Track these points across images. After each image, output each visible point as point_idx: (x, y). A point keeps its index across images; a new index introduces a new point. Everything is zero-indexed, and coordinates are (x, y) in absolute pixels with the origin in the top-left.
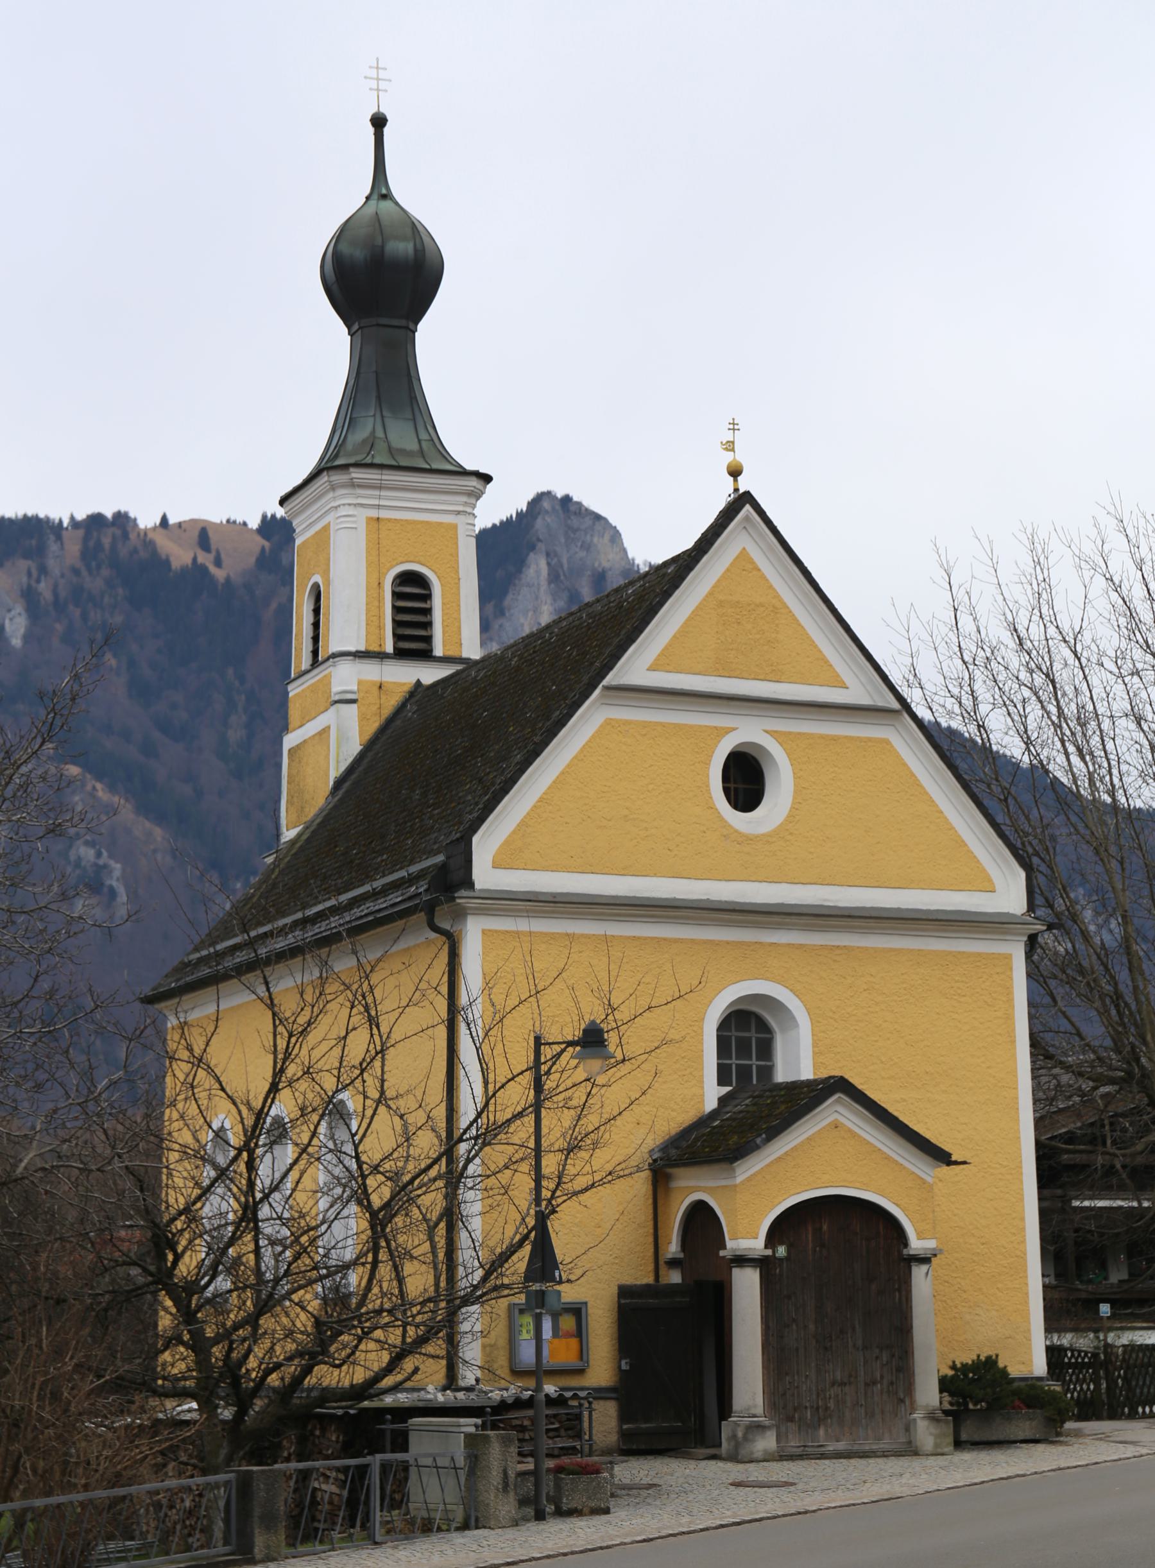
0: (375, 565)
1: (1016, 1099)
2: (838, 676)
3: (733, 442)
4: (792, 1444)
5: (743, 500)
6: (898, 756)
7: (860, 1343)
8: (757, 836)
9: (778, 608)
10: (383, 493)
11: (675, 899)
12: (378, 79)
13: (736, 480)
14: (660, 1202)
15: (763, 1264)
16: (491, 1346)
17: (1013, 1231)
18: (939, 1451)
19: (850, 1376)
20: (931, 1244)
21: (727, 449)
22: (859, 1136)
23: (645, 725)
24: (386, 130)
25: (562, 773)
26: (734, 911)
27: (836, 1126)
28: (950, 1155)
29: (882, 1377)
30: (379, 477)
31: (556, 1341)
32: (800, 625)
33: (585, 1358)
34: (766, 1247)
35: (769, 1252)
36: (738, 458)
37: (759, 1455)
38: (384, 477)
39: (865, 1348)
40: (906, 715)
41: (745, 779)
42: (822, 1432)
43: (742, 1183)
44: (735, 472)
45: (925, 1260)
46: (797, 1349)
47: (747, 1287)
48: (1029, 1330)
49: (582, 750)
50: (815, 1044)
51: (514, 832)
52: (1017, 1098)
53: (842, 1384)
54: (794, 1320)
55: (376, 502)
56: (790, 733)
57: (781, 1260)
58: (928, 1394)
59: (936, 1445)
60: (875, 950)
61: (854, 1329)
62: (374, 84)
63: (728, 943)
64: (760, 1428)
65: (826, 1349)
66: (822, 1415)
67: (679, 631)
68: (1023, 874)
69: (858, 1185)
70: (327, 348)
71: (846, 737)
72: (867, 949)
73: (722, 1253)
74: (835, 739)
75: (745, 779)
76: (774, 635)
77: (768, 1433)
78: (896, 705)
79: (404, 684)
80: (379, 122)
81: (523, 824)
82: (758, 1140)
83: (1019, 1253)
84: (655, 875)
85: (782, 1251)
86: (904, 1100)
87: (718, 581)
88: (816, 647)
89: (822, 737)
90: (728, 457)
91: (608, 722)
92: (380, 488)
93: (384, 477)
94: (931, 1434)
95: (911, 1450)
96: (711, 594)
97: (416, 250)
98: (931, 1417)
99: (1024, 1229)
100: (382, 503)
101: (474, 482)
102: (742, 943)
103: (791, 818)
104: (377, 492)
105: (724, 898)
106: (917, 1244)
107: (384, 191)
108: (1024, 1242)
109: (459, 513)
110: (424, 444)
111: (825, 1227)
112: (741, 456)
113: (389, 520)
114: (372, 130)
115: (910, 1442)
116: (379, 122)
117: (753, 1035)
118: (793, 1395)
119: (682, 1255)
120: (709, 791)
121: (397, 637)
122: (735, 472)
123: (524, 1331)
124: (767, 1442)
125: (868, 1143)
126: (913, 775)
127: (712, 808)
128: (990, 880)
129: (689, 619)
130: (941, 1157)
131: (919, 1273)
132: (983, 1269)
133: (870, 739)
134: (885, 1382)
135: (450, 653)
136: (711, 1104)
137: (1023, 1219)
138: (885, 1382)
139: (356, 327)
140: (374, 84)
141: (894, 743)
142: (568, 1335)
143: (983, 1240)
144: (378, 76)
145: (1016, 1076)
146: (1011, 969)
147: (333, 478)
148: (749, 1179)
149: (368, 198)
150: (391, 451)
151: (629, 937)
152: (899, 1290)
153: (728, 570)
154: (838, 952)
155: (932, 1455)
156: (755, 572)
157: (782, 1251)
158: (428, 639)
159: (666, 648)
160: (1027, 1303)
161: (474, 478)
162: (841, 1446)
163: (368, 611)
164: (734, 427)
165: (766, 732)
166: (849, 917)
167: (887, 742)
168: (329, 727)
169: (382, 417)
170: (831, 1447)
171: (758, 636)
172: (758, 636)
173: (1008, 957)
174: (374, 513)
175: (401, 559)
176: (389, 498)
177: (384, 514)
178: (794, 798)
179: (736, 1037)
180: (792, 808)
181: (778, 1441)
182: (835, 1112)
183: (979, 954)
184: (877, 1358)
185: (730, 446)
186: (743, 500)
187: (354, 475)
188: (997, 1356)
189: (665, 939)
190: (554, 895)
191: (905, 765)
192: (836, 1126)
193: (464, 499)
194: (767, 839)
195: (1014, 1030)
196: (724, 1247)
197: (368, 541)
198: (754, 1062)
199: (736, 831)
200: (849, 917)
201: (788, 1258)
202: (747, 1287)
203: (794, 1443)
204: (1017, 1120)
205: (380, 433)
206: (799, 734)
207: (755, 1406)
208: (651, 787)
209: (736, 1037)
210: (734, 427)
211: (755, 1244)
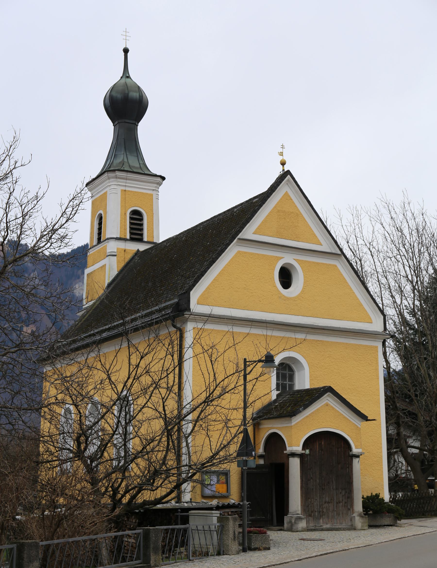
0: (124, 206)
1: (379, 399)
2: (319, 241)
3: (282, 153)
4: (311, 525)
5: (286, 174)
6: (340, 271)
7: (335, 487)
8: (291, 298)
9: (298, 214)
10: (127, 181)
11: (262, 320)
12: (126, 36)
13: (283, 167)
14: (256, 433)
15: (301, 456)
18: (363, 528)
19: (331, 500)
20: (360, 450)
21: (280, 155)
24: (129, 54)
25: (222, 270)
27: (327, 405)
28: (367, 417)
29: (342, 500)
32: (306, 221)
33: (229, 492)
34: (302, 450)
35: (303, 452)
37: (300, 529)
39: (336, 489)
41: (286, 277)
42: (321, 521)
43: (294, 425)
44: (283, 164)
45: (357, 456)
46: (313, 489)
47: (295, 465)
49: (229, 262)
50: (310, 376)
51: (205, 291)
52: (379, 399)
53: (328, 503)
54: (312, 478)
55: (125, 184)
56: (303, 261)
57: (307, 455)
58: (358, 507)
59: (362, 526)
61: (333, 482)
62: (125, 37)
64: (299, 519)
65: (323, 489)
66: (321, 514)
67: (264, 220)
69: (335, 427)
70: (105, 130)
71: (322, 263)
72: (328, 342)
73: (285, 452)
75: (286, 277)
78: (339, 252)
79: (133, 250)
80: (126, 51)
81: (208, 288)
82: (301, 409)
83: (380, 456)
84: (255, 310)
85: (307, 452)
87: (278, 202)
88: (311, 229)
89: (313, 263)
90: (281, 158)
91: (239, 252)
92: (126, 179)
94: (360, 522)
95: (353, 528)
96: (275, 207)
98: (360, 515)
99: (382, 447)
100: (127, 185)
101: (159, 179)
103: (303, 292)
104: (125, 181)
105: (279, 320)
106: (355, 450)
107: (128, 75)
108: (381, 452)
109: (154, 190)
110: (141, 165)
111: (323, 443)
112: (285, 158)
113: (129, 191)
114: (123, 54)
115: (352, 525)
116: (126, 51)
117: (287, 372)
118: (311, 507)
119: (264, 454)
120: (274, 280)
121: (131, 233)
122: (283, 164)
124: (303, 524)
125: (338, 412)
126: (345, 279)
127: (275, 286)
128: (371, 319)
129: (268, 216)
131: (355, 461)
132: (368, 462)
133: (330, 265)
134: (343, 502)
135: (150, 240)
136: (274, 397)
137: (381, 444)
138: (343, 502)
139: (117, 122)
140: (125, 37)
141: (338, 267)
142: (223, 483)
143: (368, 451)
144: (126, 35)
145: (379, 391)
146: (378, 352)
147: (109, 175)
148: (296, 424)
149: (121, 77)
150: (130, 166)
152: (348, 467)
153: (281, 199)
154: (319, 342)
155: (361, 530)
157: (307, 452)
158: (142, 235)
159: (259, 226)
160: (382, 475)
161: (159, 178)
162: (328, 526)
163: (121, 223)
164: (283, 147)
165: (294, 259)
166: (324, 329)
167: (336, 266)
168: (106, 265)
169: (127, 155)
170: (325, 526)
171: (291, 224)
172: (291, 224)
173: (377, 347)
174: (124, 188)
175: (133, 205)
176: (130, 183)
177: (127, 189)
178: (304, 285)
179: (282, 373)
180: (303, 288)
181: (306, 524)
182: (328, 399)
183: (367, 346)
184: (341, 493)
185: (281, 154)
186: (286, 174)
187: (117, 174)
188: (379, 494)
189: (258, 334)
190: (220, 316)
191: (342, 275)
192: (327, 405)
193: (155, 185)
194: (294, 299)
195: (378, 374)
196: (286, 450)
197: (122, 198)
198: (287, 382)
199: (284, 296)
200: (324, 329)
201: (310, 454)
202: (295, 465)
203: (312, 525)
204: (379, 407)
205: (126, 160)
207: (298, 510)
208: (254, 277)
209: (282, 373)
210: (283, 147)
211: (298, 448)
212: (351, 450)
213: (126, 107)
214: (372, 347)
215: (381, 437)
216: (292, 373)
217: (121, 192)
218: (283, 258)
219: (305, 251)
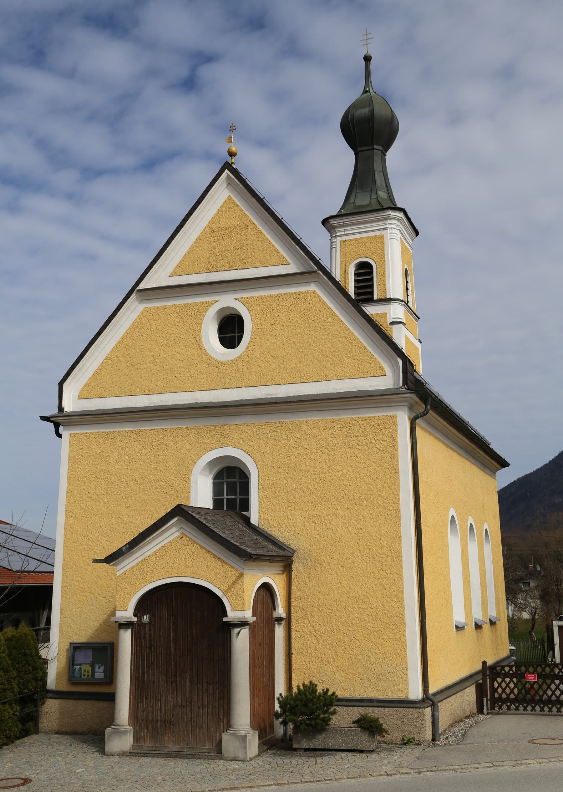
29: (208, 703)
35: (135, 619)
41: (231, 329)
55: (343, 233)
80: (367, 59)
85: (146, 618)
91: (145, 310)
100: (346, 233)
107: (368, 89)
108: (403, 607)
116: (367, 59)
135: (382, 297)
137: (402, 592)
138: (211, 707)
148: (125, 573)
157: (146, 618)
158: (372, 293)
173: (394, 417)
177: (347, 238)
200: (277, 403)
203: (147, 744)
216: (246, 480)
219: (213, 286)
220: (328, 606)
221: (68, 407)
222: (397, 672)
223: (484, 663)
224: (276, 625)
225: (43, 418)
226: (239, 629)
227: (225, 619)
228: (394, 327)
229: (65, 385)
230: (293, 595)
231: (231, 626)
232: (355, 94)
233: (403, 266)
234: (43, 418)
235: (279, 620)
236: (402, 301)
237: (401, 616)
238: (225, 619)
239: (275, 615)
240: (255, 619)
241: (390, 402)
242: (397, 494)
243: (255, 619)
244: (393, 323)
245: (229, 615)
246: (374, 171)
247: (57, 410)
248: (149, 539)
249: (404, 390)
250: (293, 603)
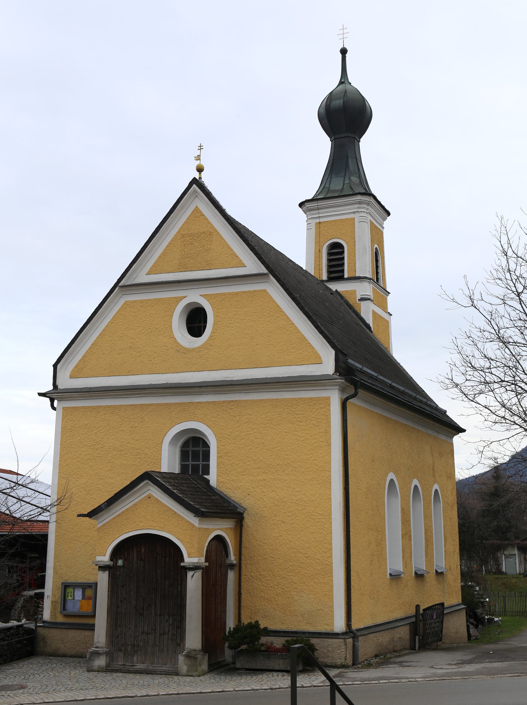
3: (200, 156)
4: (120, 663)
7: (158, 612)
11: (151, 385)
13: (200, 174)
16: (55, 602)
17: (324, 550)
18: (190, 674)
21: (197, 160)
22: (161, 502)
23: (142, 301)
26: (171, 388)
29: (169, 631)
30: (317, 204)
31: (83, 601)
34: (111, 559)
36: (202, 163)
37: (95, 668)
38: (319, 204)
39: (161, 615)
40: (271, 276)
41: (196, 321)
42: (135, 658)
44: (200, 170)
48: (332, 606)
49: (113, 318)
50: (218, 453)
52: (330, 476)
53: (148, 634)
54: (125, 599)
55: (318, 216)
56: (213, 294)
59: (188, 671)
60: (252, 401)
61: (156, 604)
63: (176, 404)
65: (140, 614)
68: (333, 352)
69: (158, 528)
72: (248, 401)
74: (236, 294)
75: (196, 321)
76: (209, 247)
77: (101, 657)
80: (344, 52)
81: (84, 356)
83: (327, 563)
84: (142, 374)
85: (120, 562)
86: (265, 480)
89: (230, 294)
90: (198, 162)
91: (126, 303)
92: (318, 209)
93: (319, 204)
94: (186, 664)
96: (178, 232)
97: (344, 102)
99: (331, 549)
102: (184, 403)
108: (331, 556)
109: (354, 212)
111: (143, 550)
112: (203, 162)
113: (325, 222)
116: (344, 52)
118: (122, 638)
123: (69, 596)
125: (165, 505)
128: (319, 357)
129: (168, 246)
130: (79, 516)
132: (306, 571)
133: (255, 291)
134: (171, 633)
137: (331, 544)
138: (171, 633)
141: (268, 291)
142: (89, 598)
143: (306, 555)
145: (330, 464)
146: (329, 405)
148: (103, 526)
151: (128, 405)
153: (188, 219)
154: (233, 404)
155: (186, 676)
156: (201, 217)
157: (120, 562)
158: (343, 271)
161: (359, 196)
163: (315, 263)
164: (201, 148)
165: (201, 295)
167: (265, 291)
169: (331, 178)
173: (328, 398)
174: (318, 221)
175: (329, 238)
176: (323, 213)
177: (322, 220)
179: (193, 451)
184: (167, 621)
185: (198, 158)
187: (307, 206)
189: (145, 405)
190: (91, 388)
193: (357, 206)
197: (316, 233)
198: (201, 463)
199: (184, 347)
201: (123, 566)
206: (217, 294)
208: (143, 331)
209: (193, 451)
212: (182, 560)
213: (345, 117)
214: (319, 399)
215: (331, 533)
216: (208, 449)
217: (316, 225)
218: (185, 297)
220: (271, 555)
221: (61, 385)
222: (325, 610)
223: (418, 606)
224: (229, 570)
225: (40, 394)
226: (193, 572)
227: (182, 564)
228: (362, 303)
229: (59, 366)
230: (243, 545)
231: (186, 569)
232: (332, 83)
233: (372, 246)
234: (40, 394)
235: (232, 566)
236: (370, 279)
237: (329, 564)
238: (182, 564)
239: (228, 562)
240: (207, 564)
241: (325, 386)
242: (329, 462)
243: (207, 564)
244: (362, 299)
245: (185, 561)
246: (347, 157)
247: (51, 388)
248: (123, 498)
249: (336, 376)
250: (243, 552)
